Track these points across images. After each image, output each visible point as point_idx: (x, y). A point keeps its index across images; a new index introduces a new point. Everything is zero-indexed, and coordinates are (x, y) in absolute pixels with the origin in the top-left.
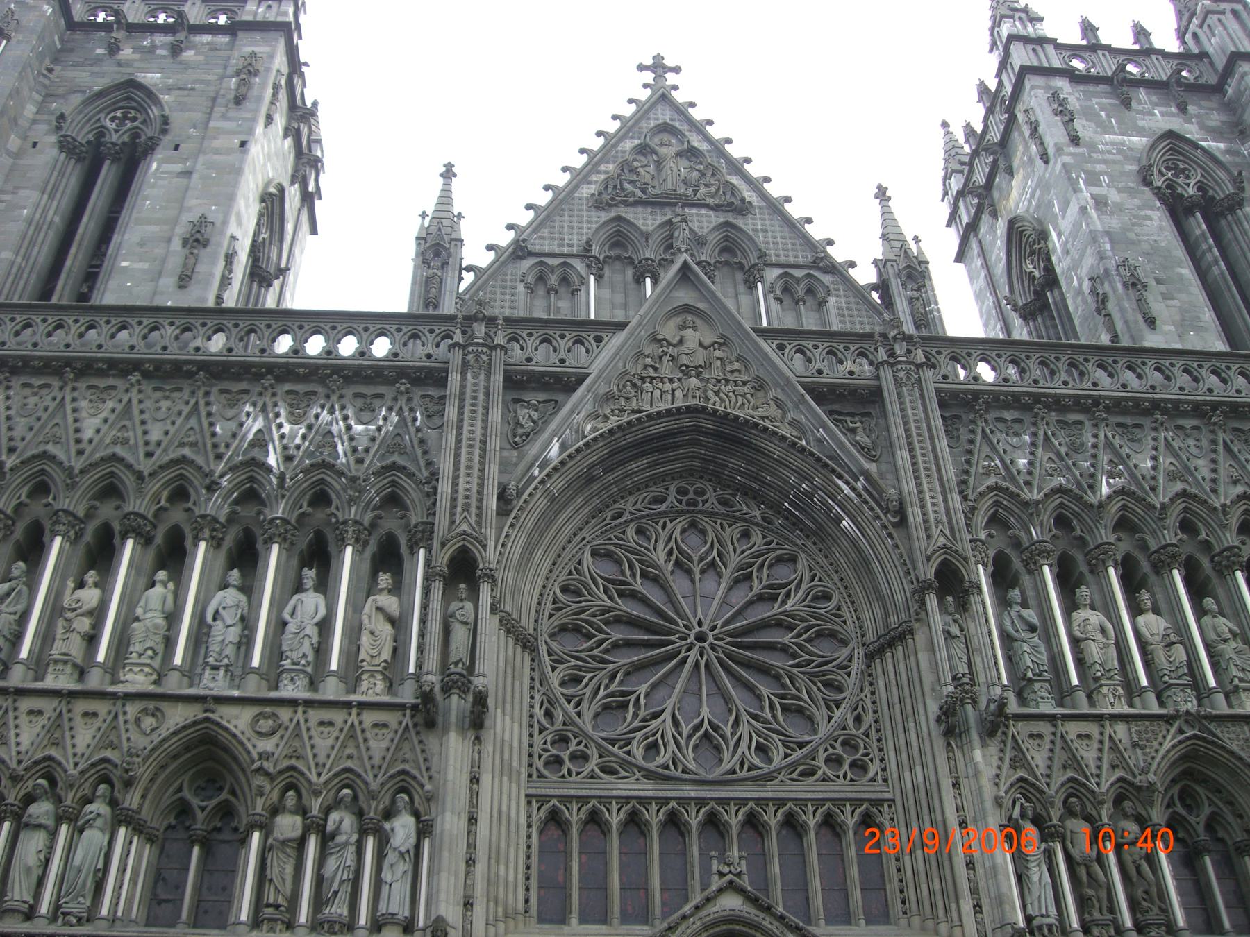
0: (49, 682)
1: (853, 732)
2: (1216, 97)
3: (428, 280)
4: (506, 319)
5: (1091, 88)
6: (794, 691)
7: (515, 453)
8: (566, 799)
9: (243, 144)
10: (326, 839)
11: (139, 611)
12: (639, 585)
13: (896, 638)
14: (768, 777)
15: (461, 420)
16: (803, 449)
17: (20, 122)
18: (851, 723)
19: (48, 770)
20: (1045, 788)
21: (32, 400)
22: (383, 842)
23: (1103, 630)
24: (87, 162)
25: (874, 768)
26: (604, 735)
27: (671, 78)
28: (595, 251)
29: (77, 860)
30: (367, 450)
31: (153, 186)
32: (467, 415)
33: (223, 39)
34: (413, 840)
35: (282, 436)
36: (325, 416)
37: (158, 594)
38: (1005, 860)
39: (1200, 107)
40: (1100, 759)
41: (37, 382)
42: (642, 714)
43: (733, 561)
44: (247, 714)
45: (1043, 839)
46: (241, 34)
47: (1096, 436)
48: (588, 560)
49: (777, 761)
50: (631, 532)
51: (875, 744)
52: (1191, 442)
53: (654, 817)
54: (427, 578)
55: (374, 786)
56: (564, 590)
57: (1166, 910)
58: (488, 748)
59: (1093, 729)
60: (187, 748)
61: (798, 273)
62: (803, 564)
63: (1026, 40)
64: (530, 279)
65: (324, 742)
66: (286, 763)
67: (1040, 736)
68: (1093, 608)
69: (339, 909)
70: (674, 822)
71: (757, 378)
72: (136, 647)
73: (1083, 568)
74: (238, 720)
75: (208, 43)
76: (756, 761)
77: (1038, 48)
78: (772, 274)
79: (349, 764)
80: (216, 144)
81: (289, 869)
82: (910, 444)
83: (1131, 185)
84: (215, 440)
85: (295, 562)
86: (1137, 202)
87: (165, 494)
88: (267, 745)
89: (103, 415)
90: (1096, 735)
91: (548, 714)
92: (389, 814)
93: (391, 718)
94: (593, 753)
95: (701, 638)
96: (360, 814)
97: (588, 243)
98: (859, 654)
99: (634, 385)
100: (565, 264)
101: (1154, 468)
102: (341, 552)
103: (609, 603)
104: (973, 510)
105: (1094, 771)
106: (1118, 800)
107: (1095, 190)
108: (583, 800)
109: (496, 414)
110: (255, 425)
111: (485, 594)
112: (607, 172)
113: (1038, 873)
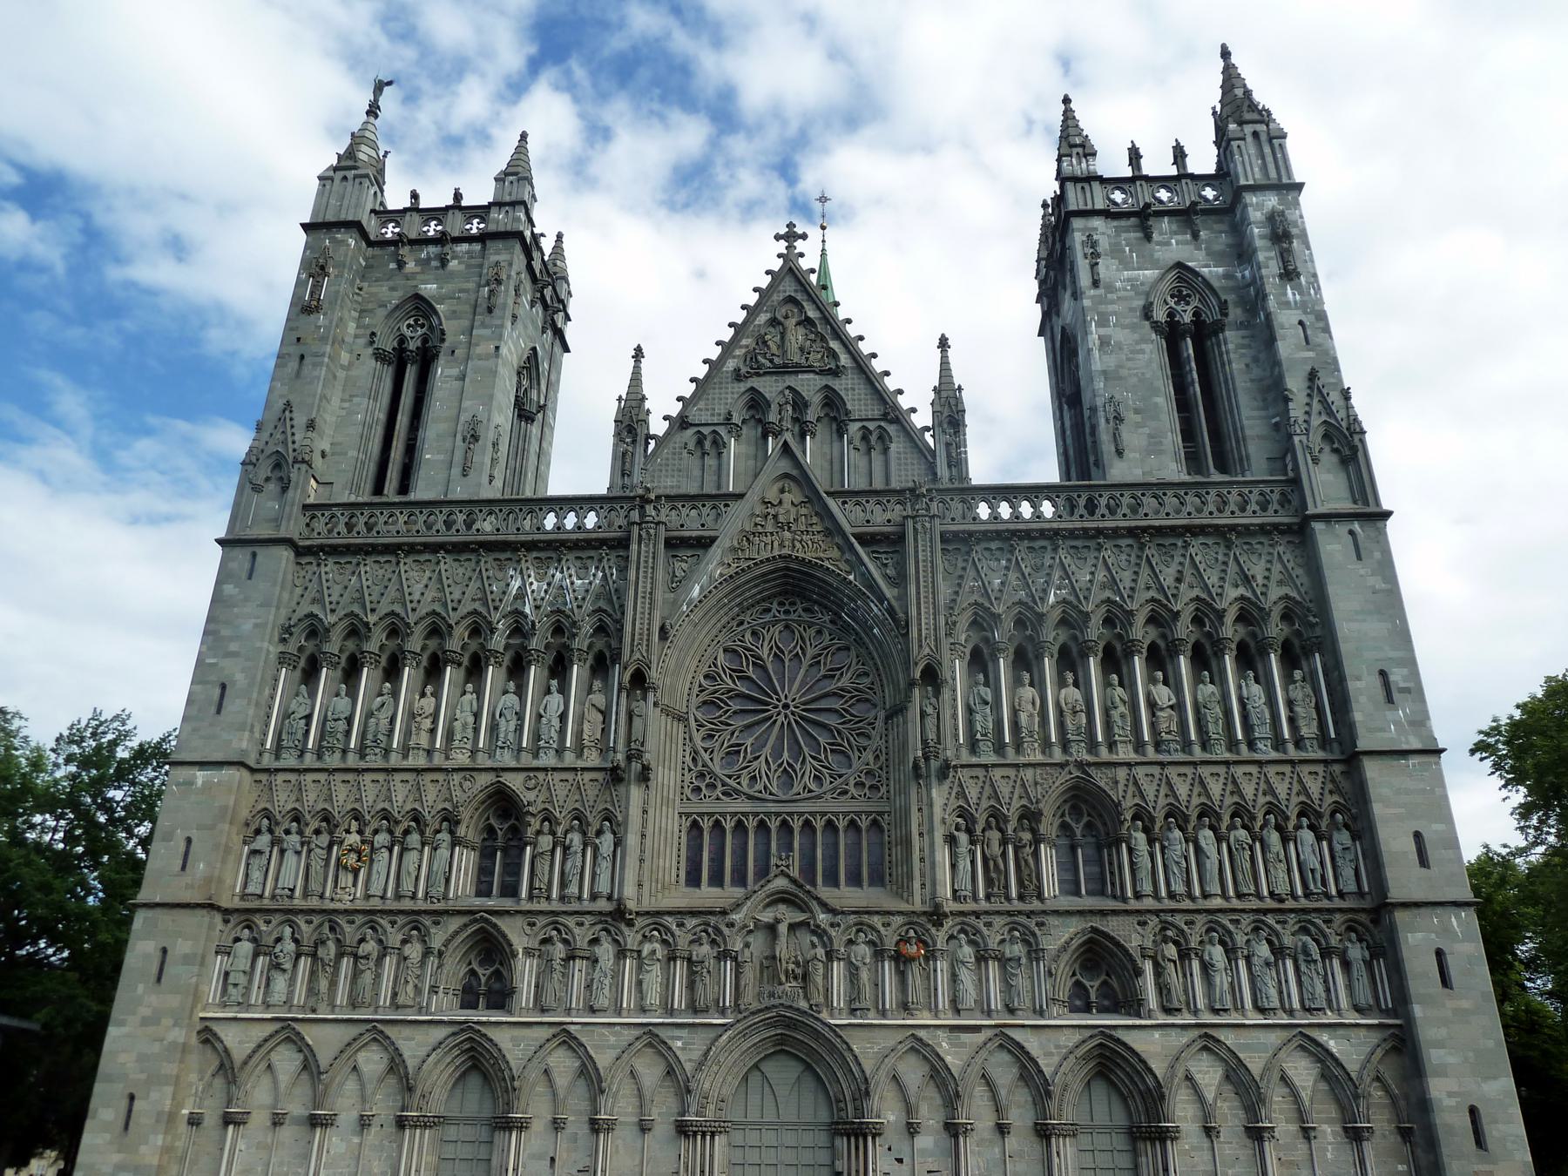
0: (411, 762)
1: (872, 766)
2: (1226, 218)
3: (624, 454)
4: (668, 497)
5: (1123, 223)
6: (840, 741)
7: (672, 595)
8: (701, 815)
9: (497, 348)
10: (566, 849)
11: (458, 711)
12: (751, 673)
13: (897, 711)
14: (819, 797)
15: (637, 578)
16: (851, 582)
17: (346, 339)
18: (872, 762)
19: (416, 817)
20: (974, 812)
21: (381, 572)
22: (596, 849)
23: (1033, 703)
24: (394, 365)
25: (883, 790)
26: (726, 772)
27: (800, 245)
28: (736, 419)
30: (584, 599)
31: (441, 389)
32: (641, 574)
33: (477, 247)
34: (612, 849)
35: (533, 592)
36: (558, 575)
37: (468, 697)
38: (943, 855)
39: (1210, 229)
40: (1012, 793)
41: (382, 559)
42: (749, 756)
43: (810, 652)
44: (522, 776)
45: (972, 842)
46: (488, 242)
47: (1053, 558)
48: (721, 656)
49: (827, 786)
50: (748, 636)
51: (884, 775)
52: (1124, 557)
53: (751, 824)
54: (619, 691)
55: (590, 819)
56: (706, 677)
57: (1039, 889)
58: (652, 792)
59: (1011, 772)
60: (489, 797)
61: (871, 426)
62: (853, 653)
63: (1075, 179)
64: (691, 446)
65: (561, 791)
66: (543, 806)
67: (977, 777)
68: (1032, 684)
69: (573, 889)
70: (762, 825)
71: (827, 529)
72: (458, 736)
73: (1031, 655)
74: (514, 782)
75: (467, 252)
76: (813, 786)
77: (1087, 186)
78: (854, 428)
79: (577, 805)
80: (478, 350)
81: (547, 868)
84: (493, 596)
85: (546, 672)
86: (1136, 336)
87: (467, 634)
88: (531, 796)
89: (425, 581)
90: (1013, 777)
91: (694, 759)
92: (599, 833)
93: (599, 776)
94: (719, 785)
95: (786, 706)
96: (584, 834)
97: (729, 416)
98: (882, 715)
99: (748, 539)
100: (714, 432)
101: (1090, 581)
102: (572, 667)
103: (733, 686)
104: (954, 623)
105: (1007, 801)
106: (1021, 818)
107: (1103, 331)
108: (711, 814)
109: (660, 574)
110: (516, 584)
111: (651, 697)
112: (747, 346)
113: (964, 864)
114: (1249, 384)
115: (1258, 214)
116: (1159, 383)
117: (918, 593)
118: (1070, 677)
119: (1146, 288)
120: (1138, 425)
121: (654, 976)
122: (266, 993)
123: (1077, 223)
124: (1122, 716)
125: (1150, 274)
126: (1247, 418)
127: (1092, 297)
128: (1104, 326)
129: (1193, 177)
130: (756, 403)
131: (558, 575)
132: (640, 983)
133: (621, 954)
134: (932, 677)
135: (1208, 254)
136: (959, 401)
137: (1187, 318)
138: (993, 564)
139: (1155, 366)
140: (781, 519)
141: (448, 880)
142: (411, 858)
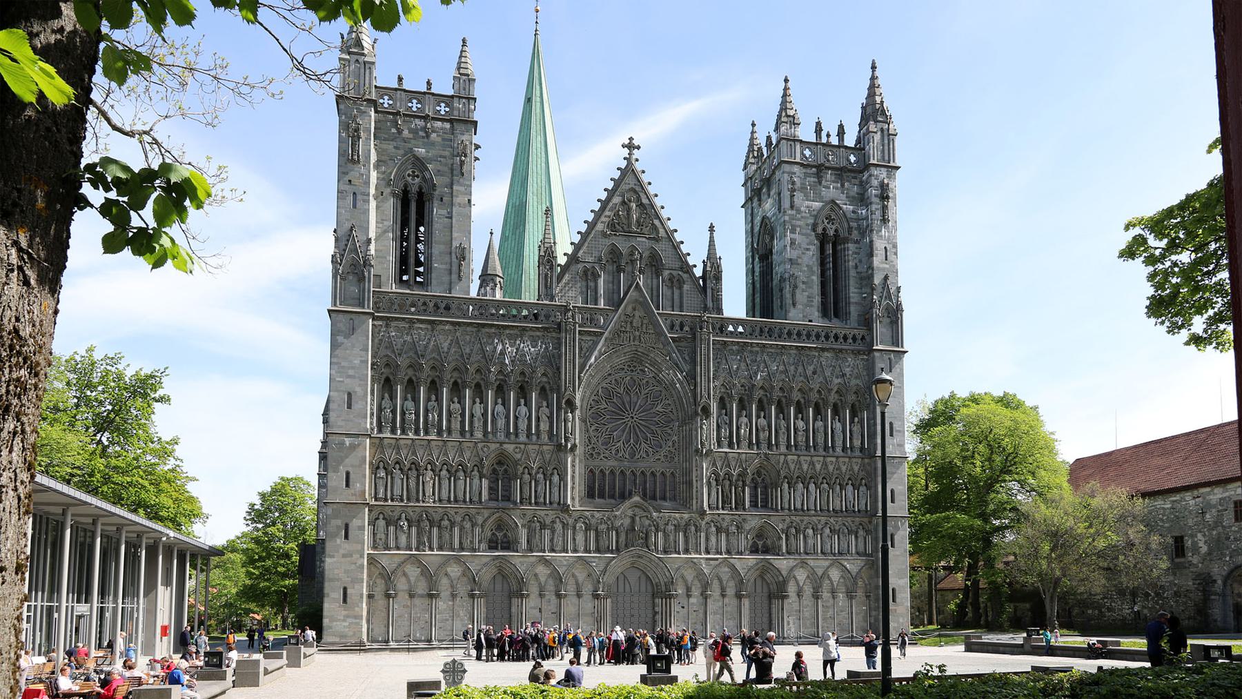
5: (808, 171)
12: (615, 401)
23: (747, 424)
25: (676, 459)
29: (474, 488)
44: (513, 446)
61: (675, 273)
63: (788, 140)
74: (510, 448)
78: (666, 273)
82: (701, 363)
83: (809, 231)
88: (518, 456)
95: (632, 418)
96: (544, 475)
100: (593, 267)
107: (793, 236)
114: (855, 275)
115: (876, 181)
116: (815, 269)
117: (701, 371)
118: (762, 414)
119: (815, 213)
120: (803, 291)
121: (580, 538)
122: (396, 543)
123: (786, 167)
124: (784, 433)
125: (817, 205)
126: (853, 293)
127: (789, 215)
128: (793, 233)
129: (846, 147)
130: (615, 253)
131: (522, 345)
132: (574, 539)
133: (565, 526)
134: (706, 411)
135: (847, 197)
136: (719, 266)
137: (832, 233)
138: (734, 357)
139: (814, 259)
140: (634, 325)
141: (480, 494)
142: (461, 483)
